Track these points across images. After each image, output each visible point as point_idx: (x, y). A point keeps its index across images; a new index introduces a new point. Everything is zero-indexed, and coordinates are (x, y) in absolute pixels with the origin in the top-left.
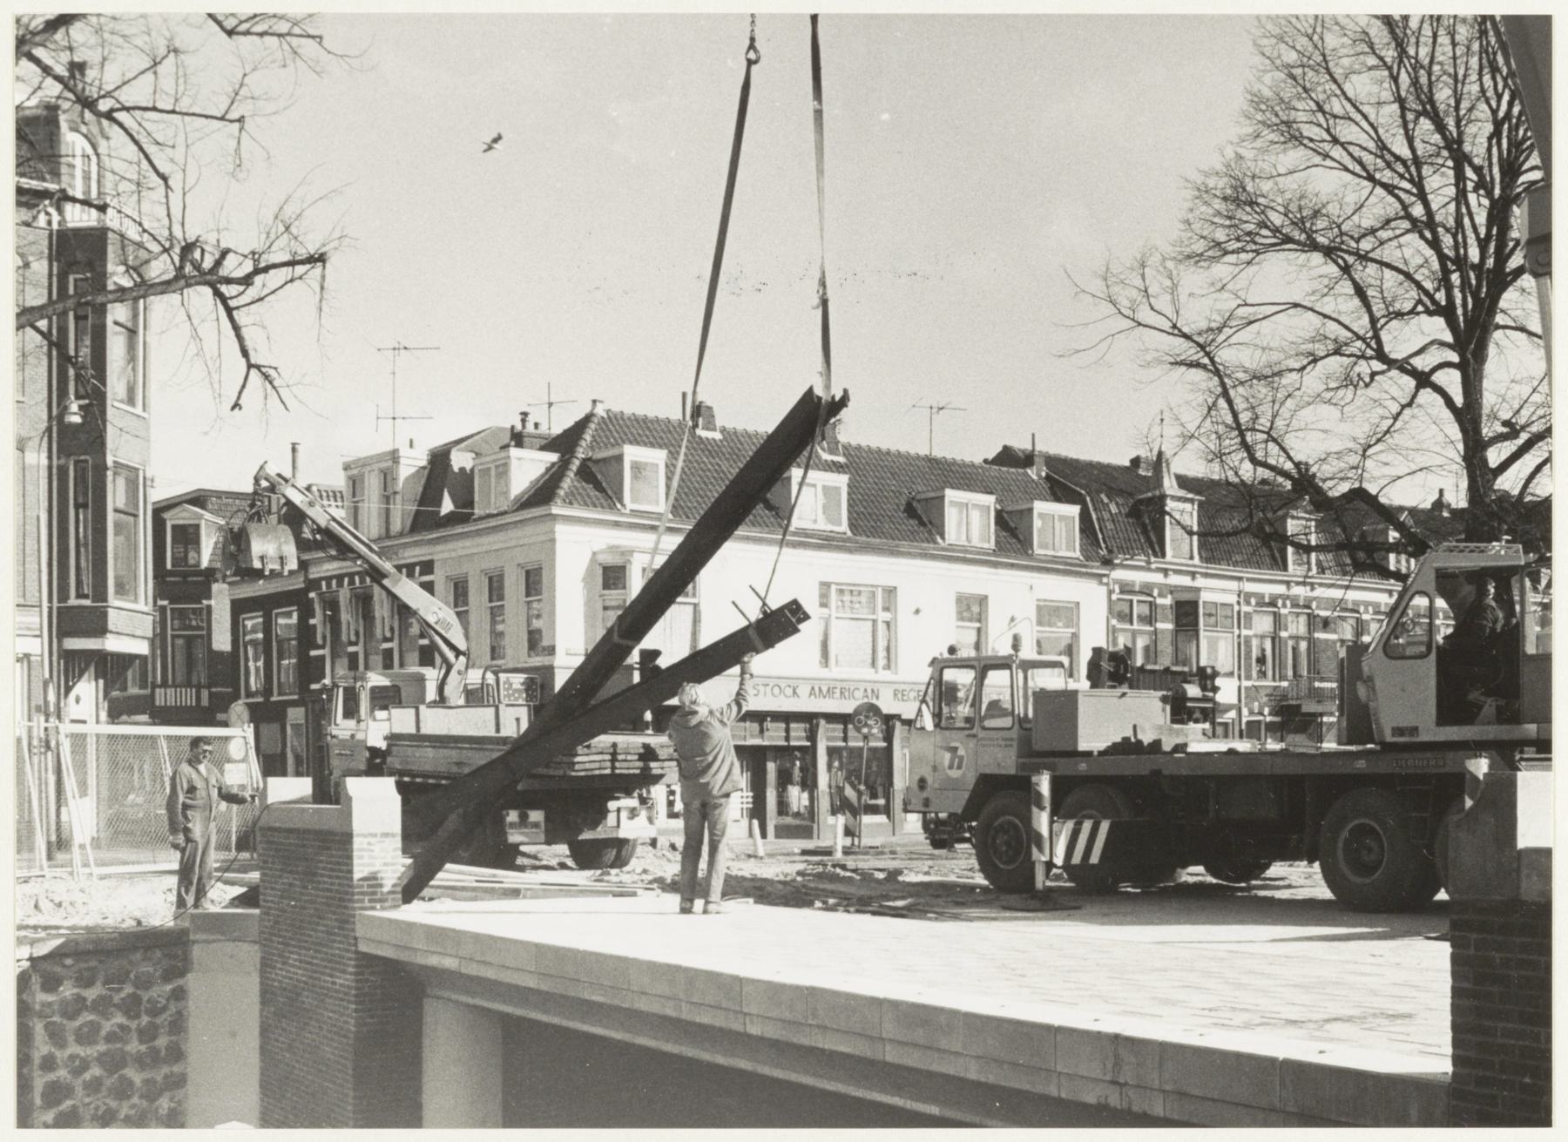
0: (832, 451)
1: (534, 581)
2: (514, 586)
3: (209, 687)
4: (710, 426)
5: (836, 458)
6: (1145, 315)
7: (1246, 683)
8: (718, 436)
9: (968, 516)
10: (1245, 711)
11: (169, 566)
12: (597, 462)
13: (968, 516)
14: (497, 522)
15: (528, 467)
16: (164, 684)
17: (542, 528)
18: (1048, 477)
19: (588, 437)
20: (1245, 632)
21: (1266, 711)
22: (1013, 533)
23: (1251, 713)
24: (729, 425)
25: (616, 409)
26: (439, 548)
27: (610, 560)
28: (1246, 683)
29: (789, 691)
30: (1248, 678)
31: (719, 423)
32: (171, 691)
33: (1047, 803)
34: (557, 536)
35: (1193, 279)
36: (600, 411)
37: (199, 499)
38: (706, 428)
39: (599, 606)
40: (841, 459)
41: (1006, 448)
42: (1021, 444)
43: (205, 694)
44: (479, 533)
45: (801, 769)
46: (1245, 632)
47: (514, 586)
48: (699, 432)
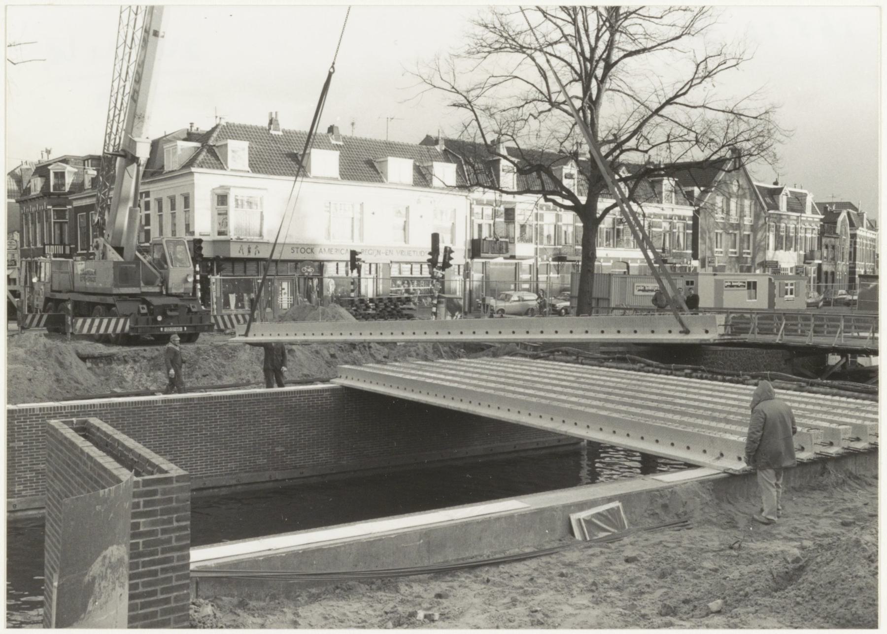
0: (337, 139)
1: (187, 200)
2: (180, 202)
3: (69, 245)
4: (277, 129)
5: (338, 143)
6: (438, 82)
7: (540, 246)
8: (280, 133)
9: (400, 169)
10: (539, 259)
11: (52, 190)
12: (217, 147)
13: (400, 169)
14: (173, 176)
15: (186, 148)
16: (50, 244)
17: (188, 178)
18: (445, 150)
19: (215, 135)
20: (539, 223)
21: (550, 259)
22: (423, 177)
23: (542, 260)
24: (287, 128)
25: (231, 121)
26: (151, 186)
27: (220, 192)
28: (540, 246)
29: (309, 251)
30: (541, 243)
31: (281, 127)
32: (52, 247)
33: (71, 312)
34: (195, 181)
35: (471, 62)
36: (223, 123)
37: (65, 160)
38: (274, 130)
39: (216, 213)
40: (341, 143)
41: (427, 136)
42: (434, 134)
43: (68, 248)
44: (165, 179)
45: (201, 290)
46: (539, 223)
47: (180, 202)
48: (272, 132)
